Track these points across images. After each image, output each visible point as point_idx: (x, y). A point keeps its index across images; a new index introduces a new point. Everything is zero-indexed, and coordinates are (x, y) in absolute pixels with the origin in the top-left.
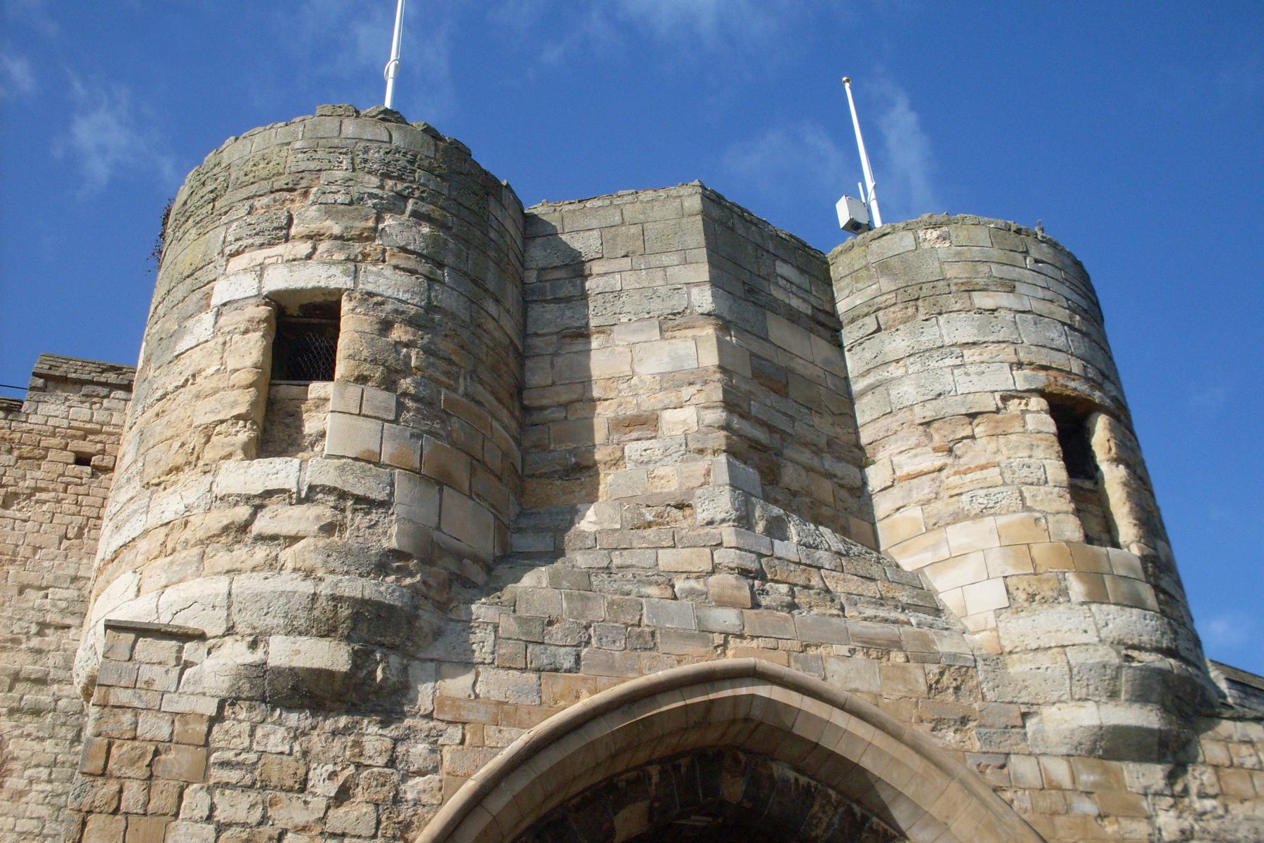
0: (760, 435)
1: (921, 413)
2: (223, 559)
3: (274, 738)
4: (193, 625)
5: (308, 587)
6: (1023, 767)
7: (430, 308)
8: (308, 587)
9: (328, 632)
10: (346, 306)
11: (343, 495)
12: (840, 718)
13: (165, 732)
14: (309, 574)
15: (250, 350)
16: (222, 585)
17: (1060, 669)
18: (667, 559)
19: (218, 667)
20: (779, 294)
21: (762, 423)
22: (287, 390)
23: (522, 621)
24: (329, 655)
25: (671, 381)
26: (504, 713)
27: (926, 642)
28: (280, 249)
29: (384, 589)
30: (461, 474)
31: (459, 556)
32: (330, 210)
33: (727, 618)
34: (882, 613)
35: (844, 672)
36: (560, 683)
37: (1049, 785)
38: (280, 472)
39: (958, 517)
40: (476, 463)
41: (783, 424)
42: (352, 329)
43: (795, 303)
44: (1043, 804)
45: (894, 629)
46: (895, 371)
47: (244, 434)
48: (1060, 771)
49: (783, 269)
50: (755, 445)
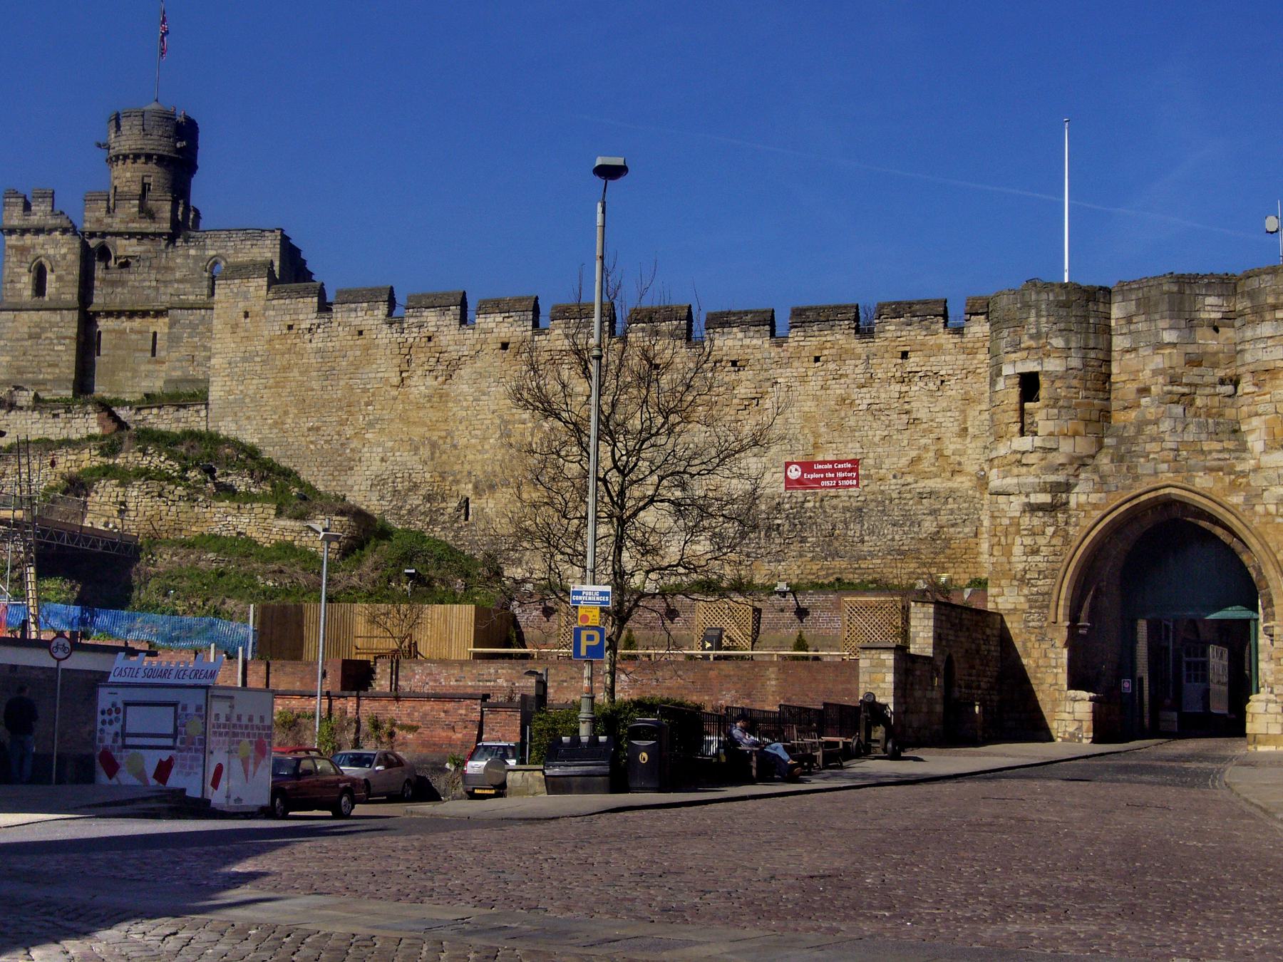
0: (1186, 390)
1: (1252, 368)
2: (1015, 470)
3: (1036, 521)
4: (1011, 491)
5: (1037, 480)
6: (1260, 509)
7: (1067, 370)
8: (1037, 480)
9: (1045, 491)
10: (1041, 378)
11: (1044, 449)
12: (1197, 498)
13: (1008, 522)
14: (1037, 476)
15: (1015, 393)
16: (1015, 480)
17: (1275, 475)
18: (1149, 447)
19: (1017, 502)
20: (1204, 315)
21: (1187, 385)
22: (1028, 405)
23: (1101, 477)
24: (1045, 498)
25: (1155, 372)
26: (1095, 506)
27: (1233, 466)
28: (1018, 354)
29: (1060, 477)
30: (1081, 428)
31: (1081, 458)
32: (1031, 337)
33: (1165, 466)
34: (1221, 456)
35: (1202, 481)
36: (1112, 496)
37: (1268, 514)
38: (1026, 443)
39: (1257, 414)
40: (1087, 422)
41: (1197, 380)
42: (1044, 382)
43: (1213, 315)
44: (1264, 520)
45: (1221, 463)
46: (1247, 346)
47: (1016, 428)
48: (1272, 509)
49: (1210, 300)
50: (1183, 395)
